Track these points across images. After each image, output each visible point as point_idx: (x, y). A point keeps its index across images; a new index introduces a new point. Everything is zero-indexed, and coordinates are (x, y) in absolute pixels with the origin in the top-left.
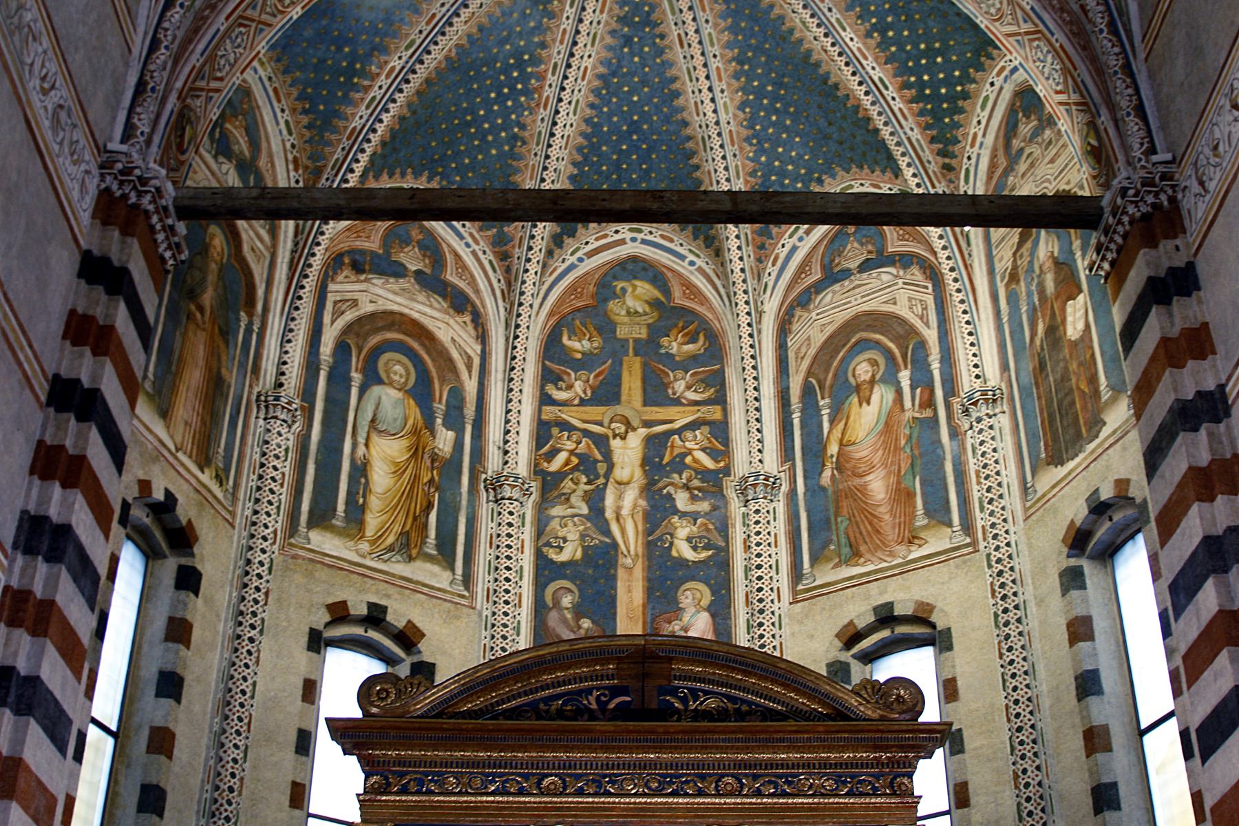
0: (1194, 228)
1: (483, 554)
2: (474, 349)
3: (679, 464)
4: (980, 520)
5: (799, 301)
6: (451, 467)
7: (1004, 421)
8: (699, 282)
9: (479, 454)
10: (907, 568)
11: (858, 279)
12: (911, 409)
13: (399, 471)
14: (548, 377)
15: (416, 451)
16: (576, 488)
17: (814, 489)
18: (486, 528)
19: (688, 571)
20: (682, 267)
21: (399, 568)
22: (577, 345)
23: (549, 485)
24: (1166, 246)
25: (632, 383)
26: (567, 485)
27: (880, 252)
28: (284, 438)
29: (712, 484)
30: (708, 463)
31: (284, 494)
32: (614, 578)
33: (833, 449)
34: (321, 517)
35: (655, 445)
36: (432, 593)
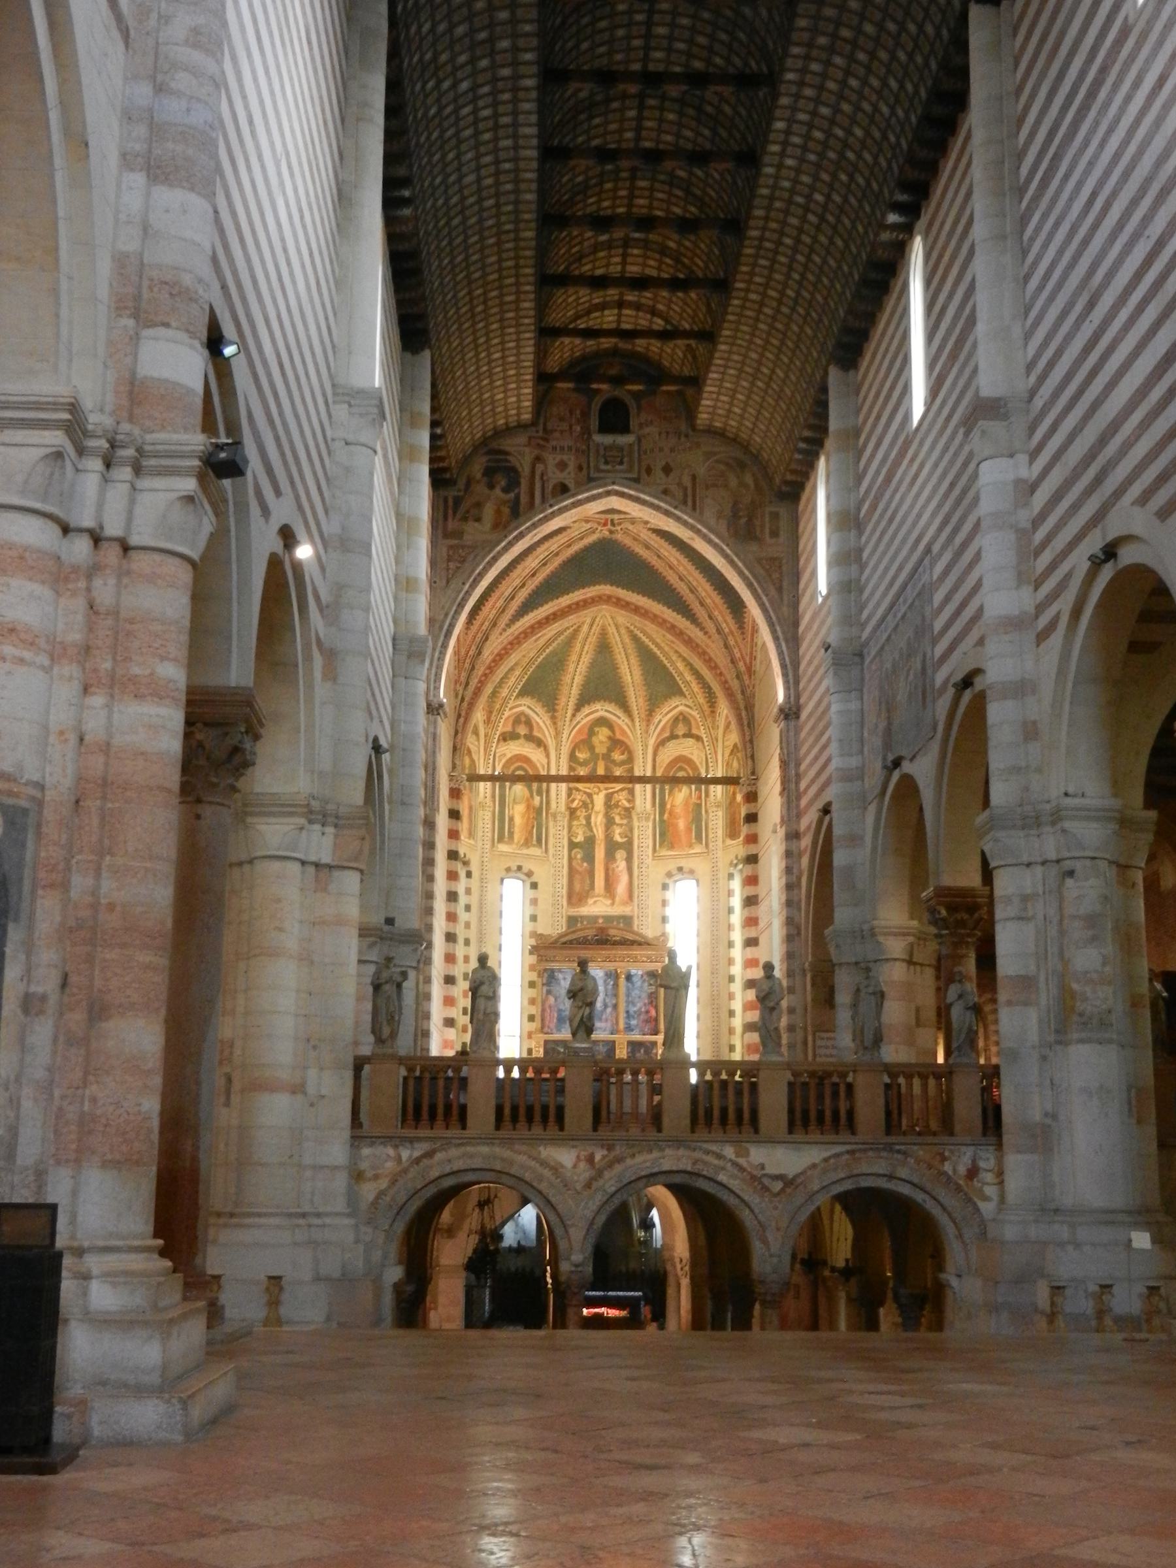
0: (760, 800)
2: (545, 761)
3: (617, 805)
4: (711, 845)
5: (662, 743)
6: (539, 811)
7: (720, 813)
8: (625, 728)
9: (548, 803)
10: (688, 856)
11: (682, 740)
12: (694, 799)
13: (523, 817)
15: (528, 807)
16: (582, 814)
17: (662, 821)
18: (552, 831)
20: (620, 722)
21: (525, 851)
22: (582, 756)
23: (572, 812)
24: (753, 804)
26: (578, 813)
27: (690, 730)
28: (488, 815)
29: (628, 812)
30: (627, 805)
31: (489, 834)
32: (593, 849)
33: (668, 806)
34: (501, 839)
35: (609, 797)
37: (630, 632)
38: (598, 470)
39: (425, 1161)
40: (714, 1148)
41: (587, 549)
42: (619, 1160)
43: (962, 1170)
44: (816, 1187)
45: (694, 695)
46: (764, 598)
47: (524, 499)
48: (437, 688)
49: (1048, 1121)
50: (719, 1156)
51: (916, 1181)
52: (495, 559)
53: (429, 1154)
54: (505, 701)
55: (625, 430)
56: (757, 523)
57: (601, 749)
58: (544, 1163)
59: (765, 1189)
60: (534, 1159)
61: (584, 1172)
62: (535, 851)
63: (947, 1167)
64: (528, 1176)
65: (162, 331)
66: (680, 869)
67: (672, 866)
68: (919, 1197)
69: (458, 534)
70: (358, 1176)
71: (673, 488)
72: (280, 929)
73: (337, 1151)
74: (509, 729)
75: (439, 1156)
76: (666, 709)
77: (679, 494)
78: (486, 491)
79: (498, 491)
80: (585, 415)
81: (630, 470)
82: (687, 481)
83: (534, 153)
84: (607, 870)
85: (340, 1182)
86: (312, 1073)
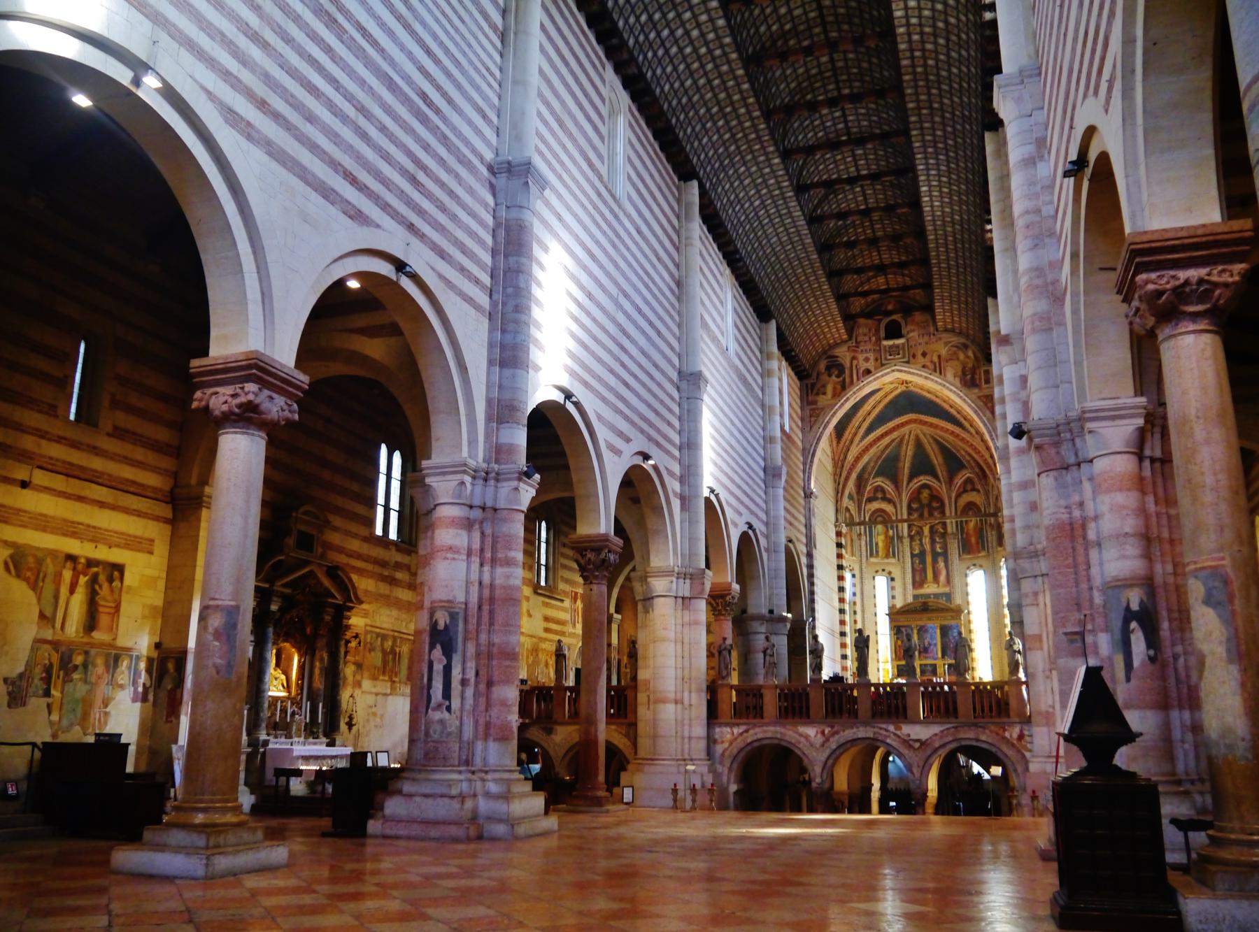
1: (901, 554)
2: (894, 511)
3: (936, 532)
5: (958, 496)
7: (994, 533)
14: (909, 514)
16: (917, 538)
18: (901, 549)
19: (939, 554)
21: (886, 561)
22: (915, 506)
23: (911, 538)
25: (926, 514)
29: (944, 535)
34: (871, 555)
35: (932, 528)
36: (892, 564)
37: (932, 437)
38: (886, 359)
39: (745, 735)
40: (884, 726)
41: (897, 397)
42: (837, 733)
43: (1015, 735)
44: (937, 745)
45: (972, 468)
46: (985, 419)
47: (847, 380)
48: (809, 484)
49: (1051, 710)
50: (886, 730)
51: (990, 741)
52: (835, 413)
53: (747, 731)
54: (867, 480)
55: (900, 336)
56: (977, 377)
57: (925, 501)
58: (801, 735)
59: (911, 747)
60: (797, 732)
61: (820, 739)
62: (892, 560)
63: (1007, 734)
64: (793, 741)
65: (506, 425)
66: (974, 565)
67: (969, 563)
68: (994, 750)
69: (815, 403)
70: (711, 741)
71: (929, 364)
72: (665, 629)
73: (700, 730)
74: (871, 495)
75: (751, 732)
76: (960, 476)
77: (932, 367)
78: (827, 378)
79: (834, 378)
80: (877, 331)
81: (904, 357)
82: (936, 359)
83: (803, 223)
84: (934, 567)
85: (702, 744)
86: (686, 694)
